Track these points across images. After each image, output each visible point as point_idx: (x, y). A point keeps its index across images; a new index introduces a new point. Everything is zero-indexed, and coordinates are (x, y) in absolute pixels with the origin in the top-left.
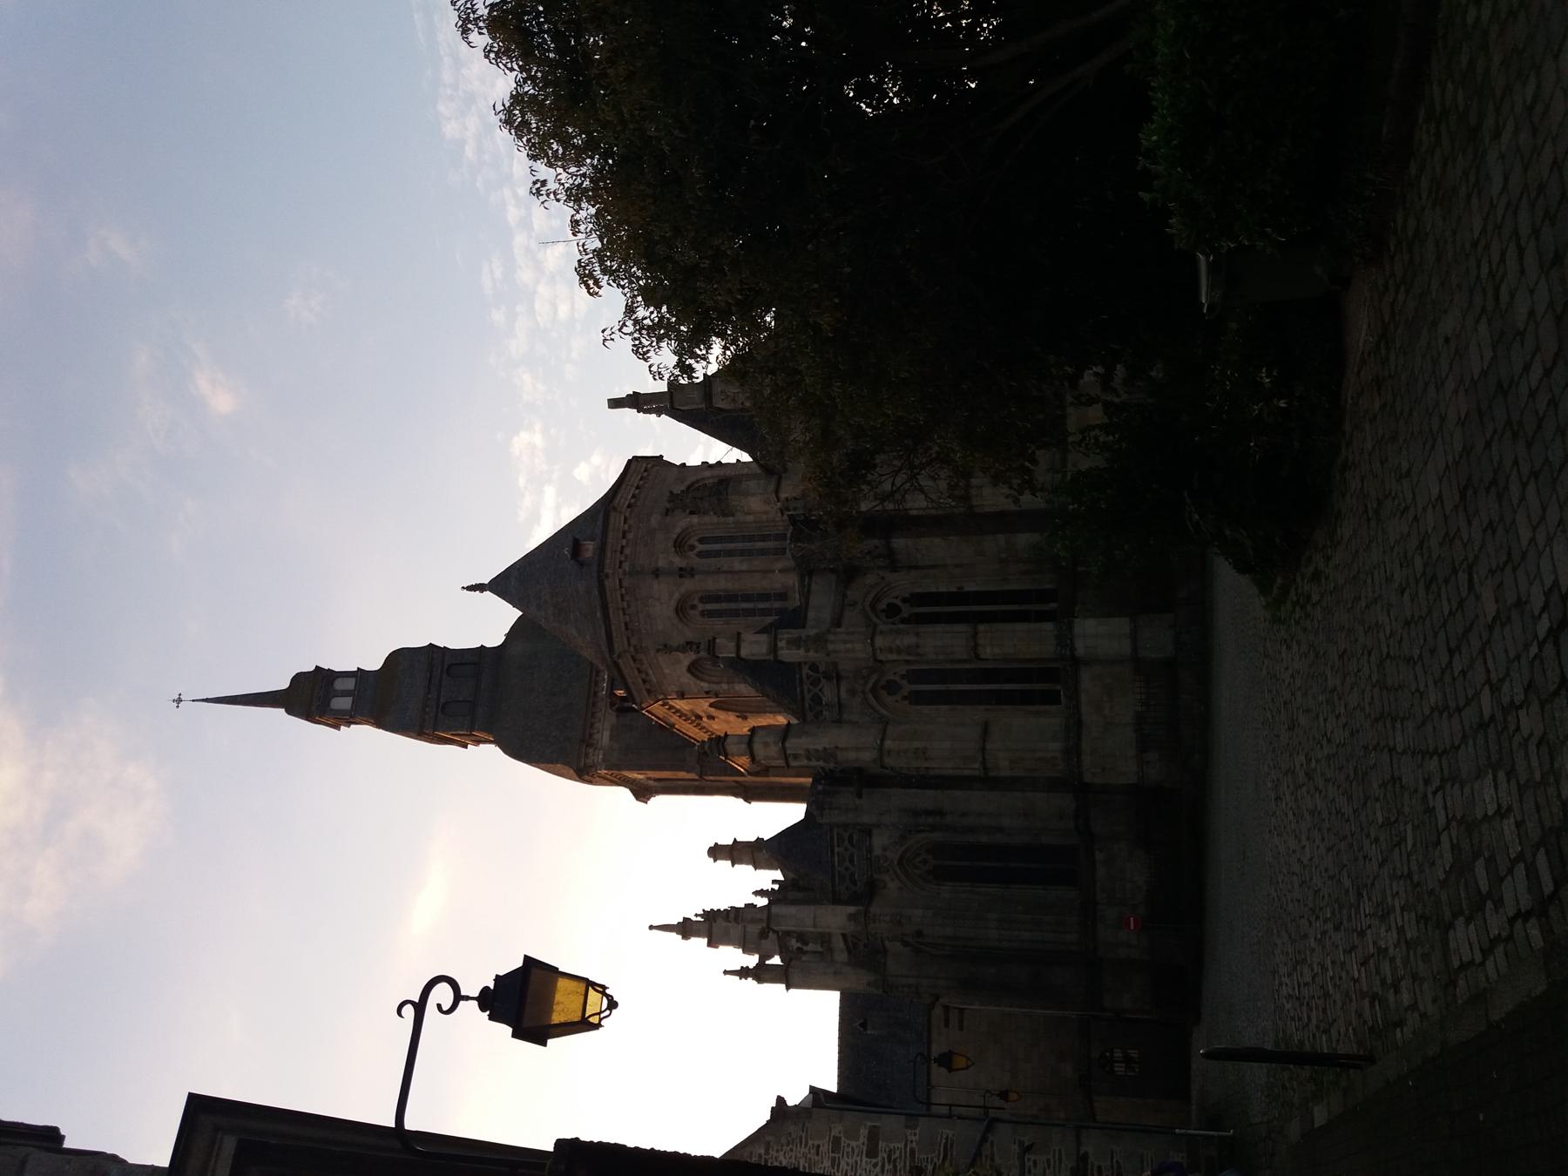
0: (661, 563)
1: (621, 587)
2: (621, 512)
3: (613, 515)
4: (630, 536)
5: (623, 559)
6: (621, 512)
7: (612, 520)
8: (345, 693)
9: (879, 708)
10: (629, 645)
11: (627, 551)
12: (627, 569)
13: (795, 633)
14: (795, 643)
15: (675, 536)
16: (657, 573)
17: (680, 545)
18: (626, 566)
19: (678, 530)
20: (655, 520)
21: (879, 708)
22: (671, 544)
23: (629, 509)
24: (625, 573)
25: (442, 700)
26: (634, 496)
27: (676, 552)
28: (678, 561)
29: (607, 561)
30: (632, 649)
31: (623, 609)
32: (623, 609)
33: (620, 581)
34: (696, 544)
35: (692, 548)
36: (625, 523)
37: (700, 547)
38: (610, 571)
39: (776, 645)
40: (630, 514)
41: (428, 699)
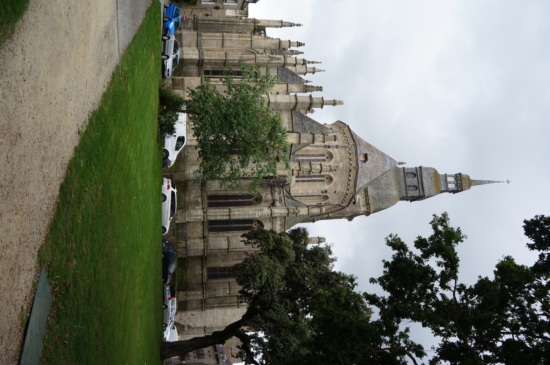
0: (336, 150)
1: (348, 143)
2: (353, 167)
3: (355, 166)
4: (348, 160)
5: (349, 151)
6: (353, 167)
7: (355, 164)
8: (450, 183)
9: (253, 51)
10: (343, 130)
11: (348, 155)
12: (347, 148)
13: (279, 61)
14: (278, 59)
15: (333, 159)
16: (337, 147)
17: (331, 156)
18: (348, 149)
19: (332, 161)
20: (341, 165)
21: (253, 51)
22: (334, 156)
23: (351, 169)
24: (348, 147)
25: (416, 178)
26: (350, 176)
27: (332, 154)
28: (330, 150)
29: (354, 150)
30: (342, 128)
31: (346, 137)
32: (346, 137)
33: (349, 144)
34: (326, 159)
35: (327, 158)
36: (351, 164)
37: (324, 158)
38: (352, 146)
39: (285, 59)
40: (350, 168)
41: (421, 178)
